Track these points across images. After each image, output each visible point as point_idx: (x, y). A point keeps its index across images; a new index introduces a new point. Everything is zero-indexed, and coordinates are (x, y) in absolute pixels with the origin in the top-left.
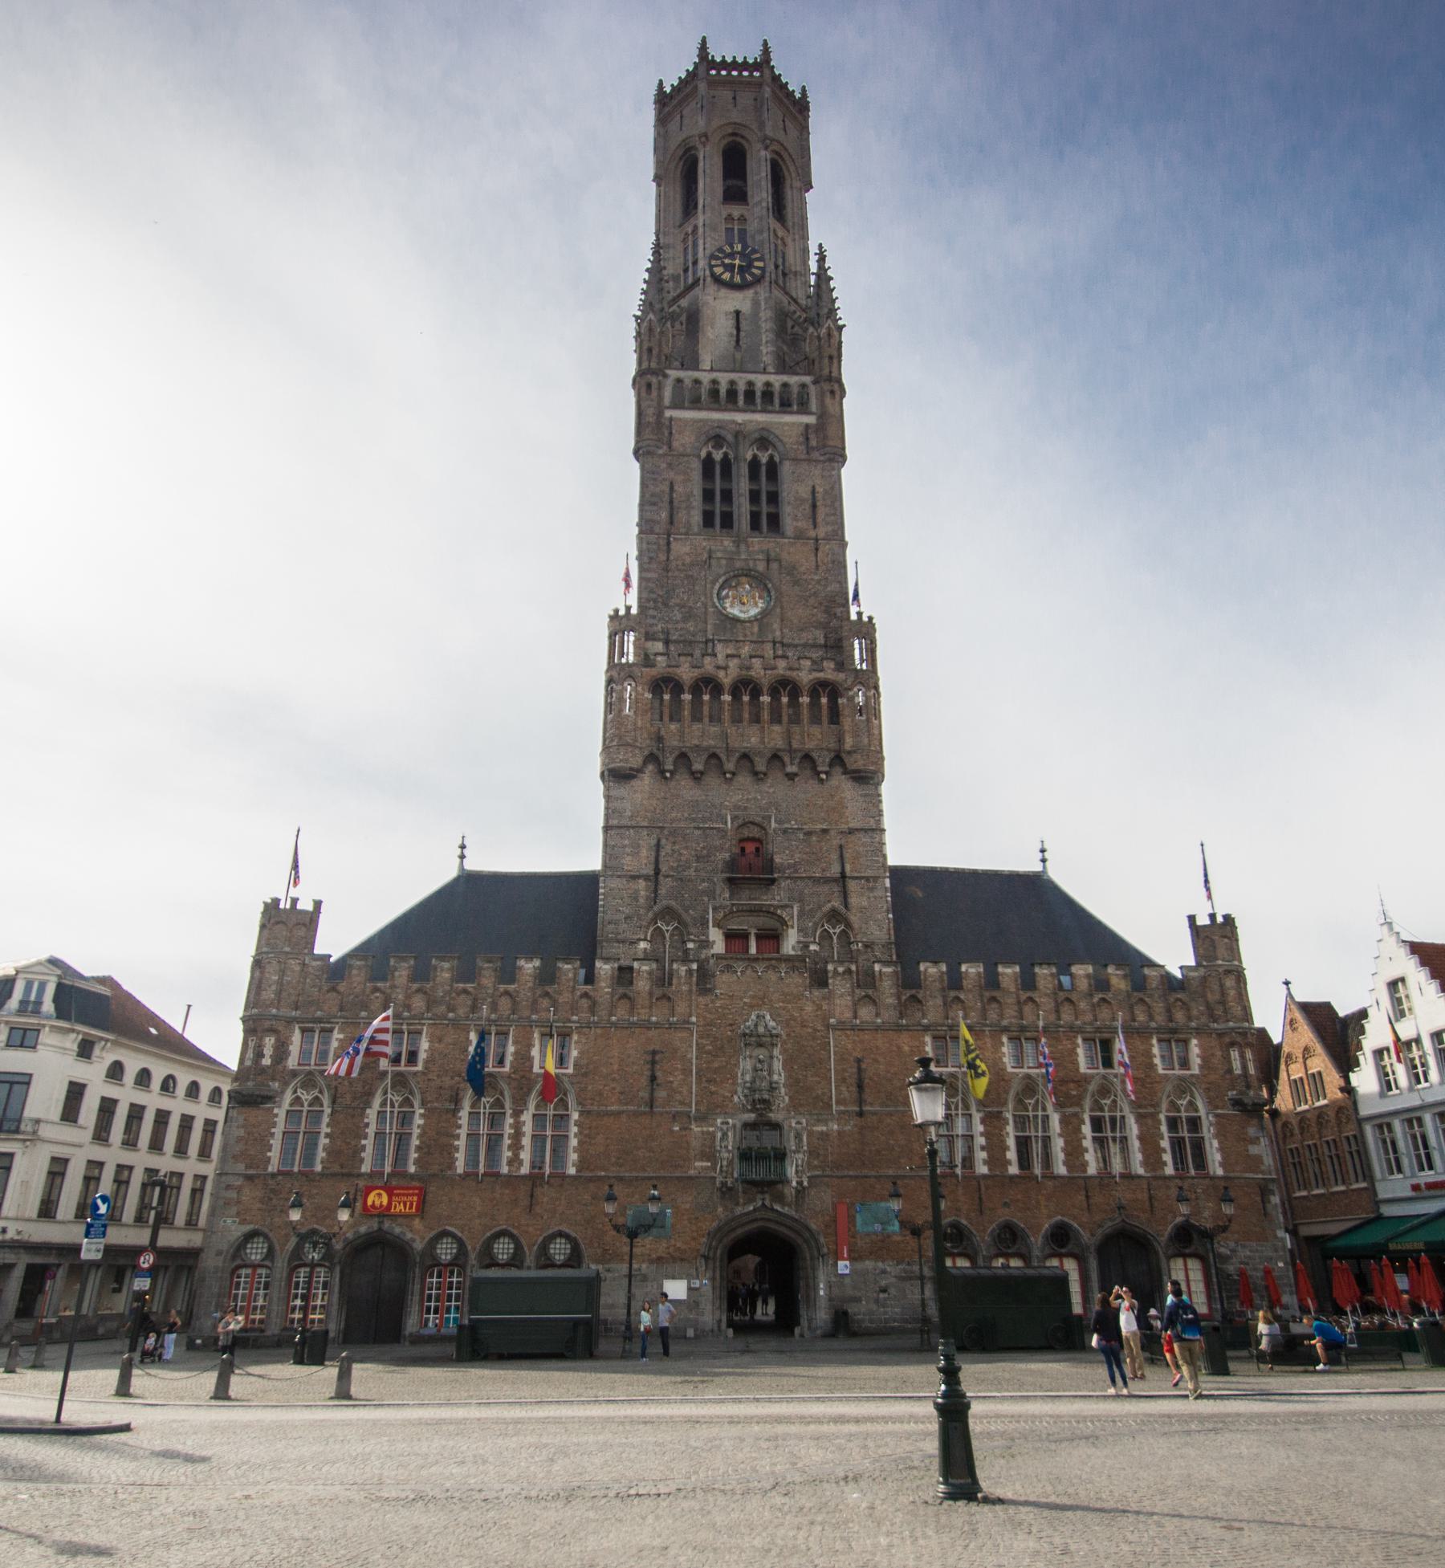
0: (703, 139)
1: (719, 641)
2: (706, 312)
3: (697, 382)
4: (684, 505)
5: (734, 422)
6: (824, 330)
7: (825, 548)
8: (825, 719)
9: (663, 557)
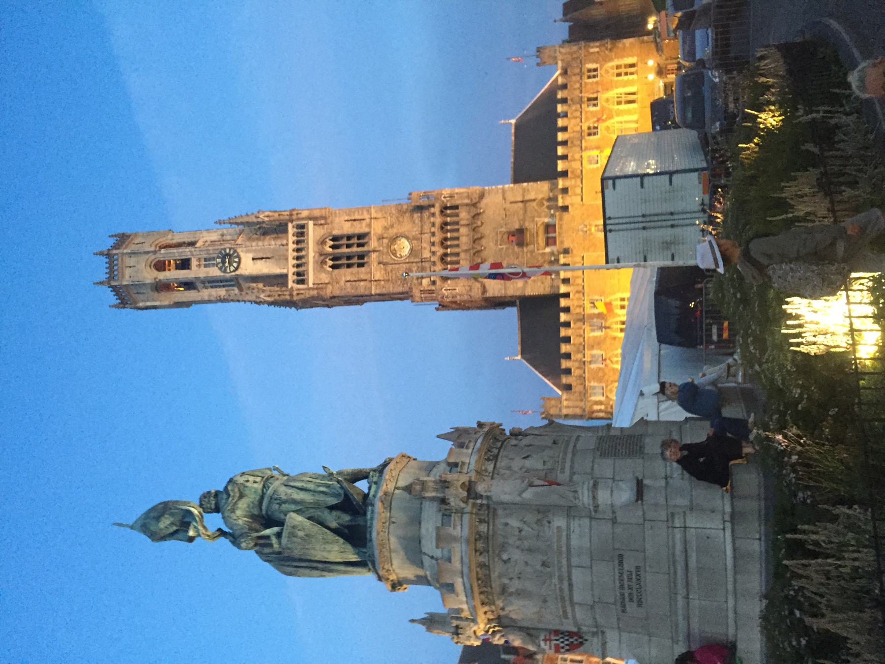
3: (293, 274)
5: (314, 257)
7: (374, 215)
8: (457, 211)
9: (382, 283)
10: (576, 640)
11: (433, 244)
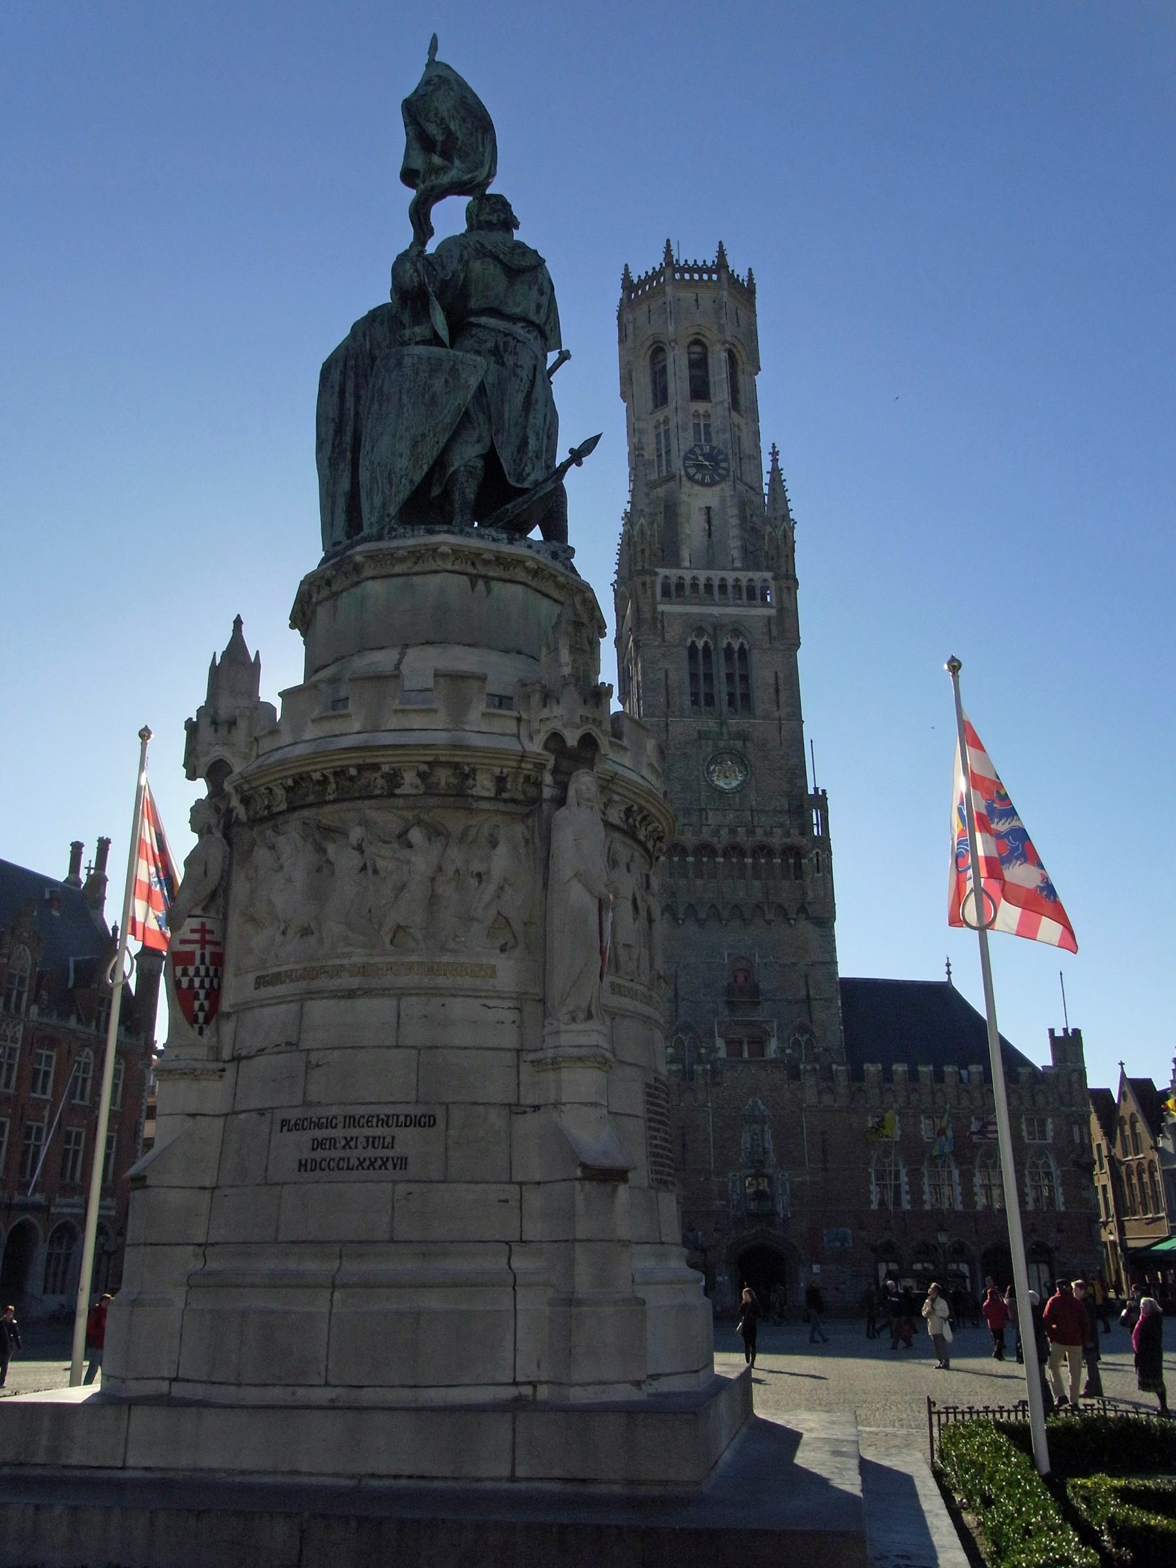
0: (673, 344)
1: (711, 810)
2: (683, 509)
3: (680, 578)
4: (676, 692)
5: (711, 615)
6: (780, 533)
10: (201, 1007)
11: (733, 831)
